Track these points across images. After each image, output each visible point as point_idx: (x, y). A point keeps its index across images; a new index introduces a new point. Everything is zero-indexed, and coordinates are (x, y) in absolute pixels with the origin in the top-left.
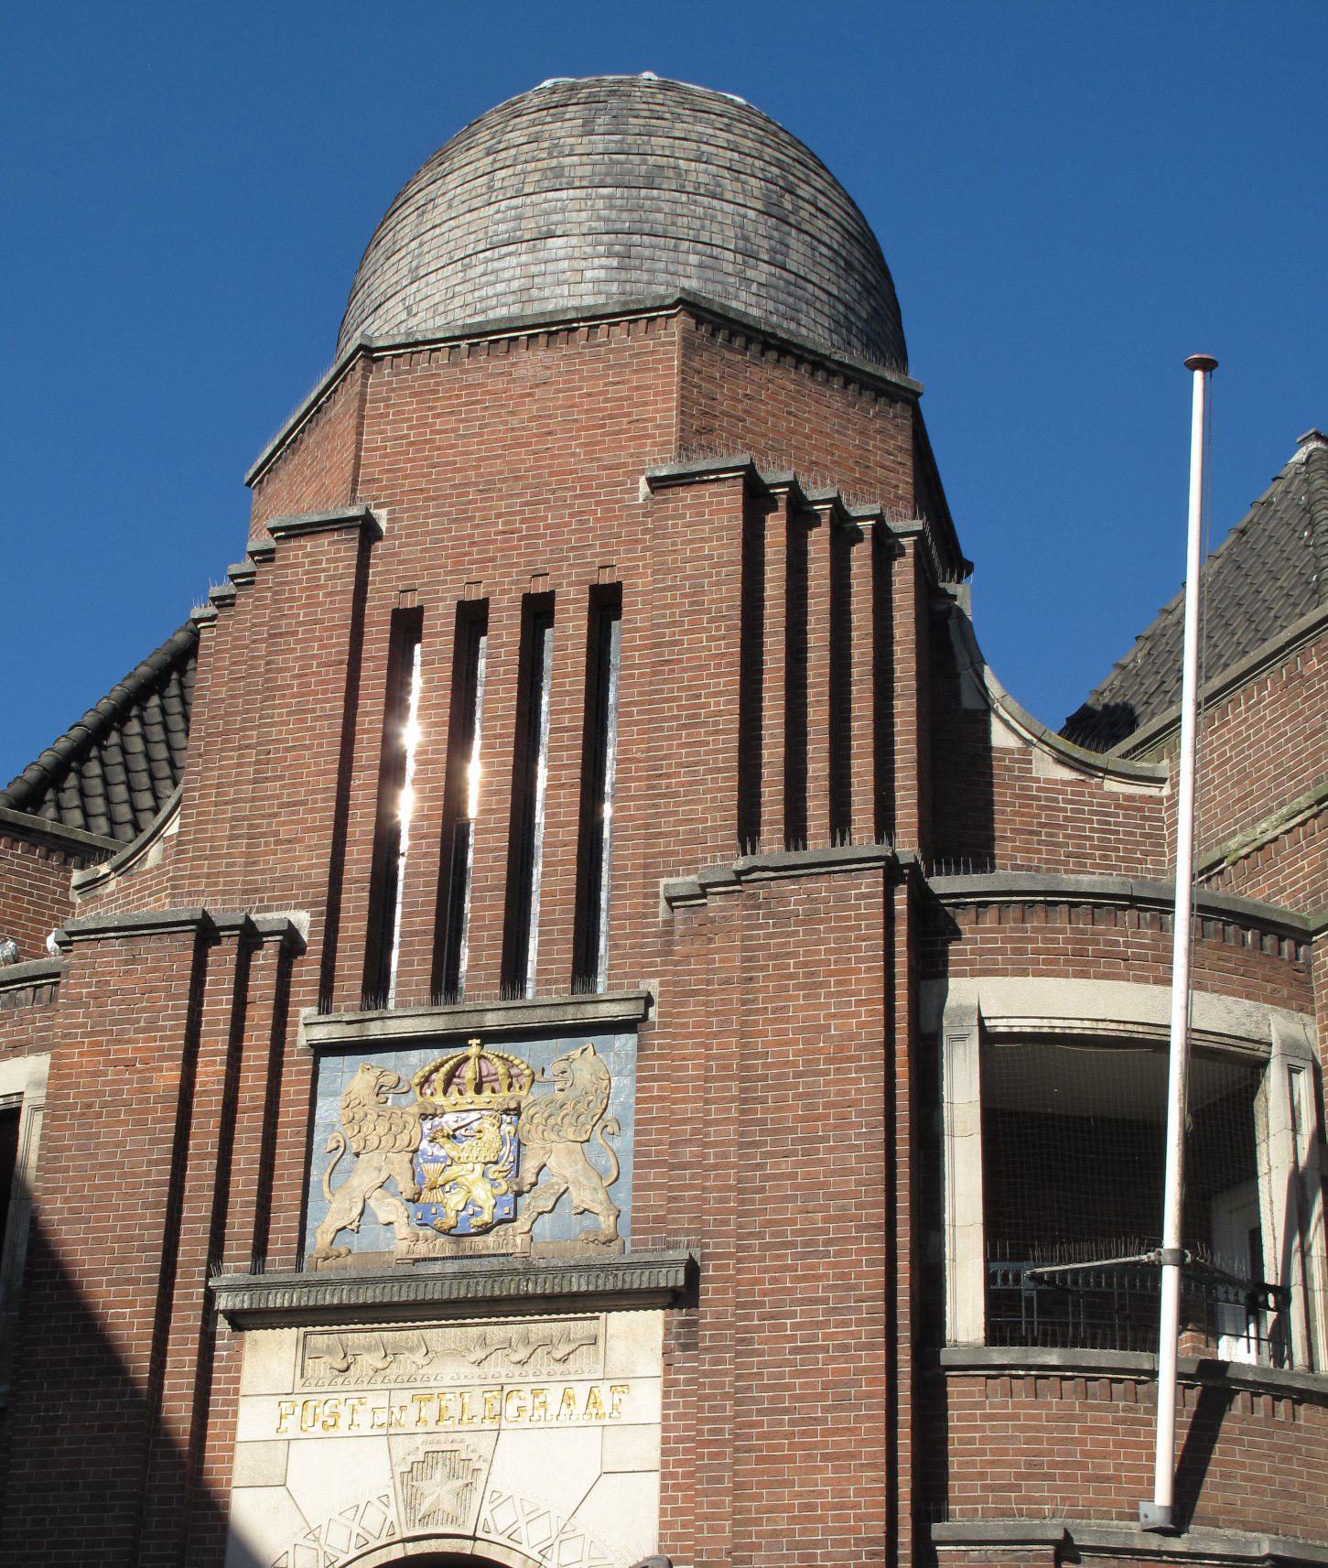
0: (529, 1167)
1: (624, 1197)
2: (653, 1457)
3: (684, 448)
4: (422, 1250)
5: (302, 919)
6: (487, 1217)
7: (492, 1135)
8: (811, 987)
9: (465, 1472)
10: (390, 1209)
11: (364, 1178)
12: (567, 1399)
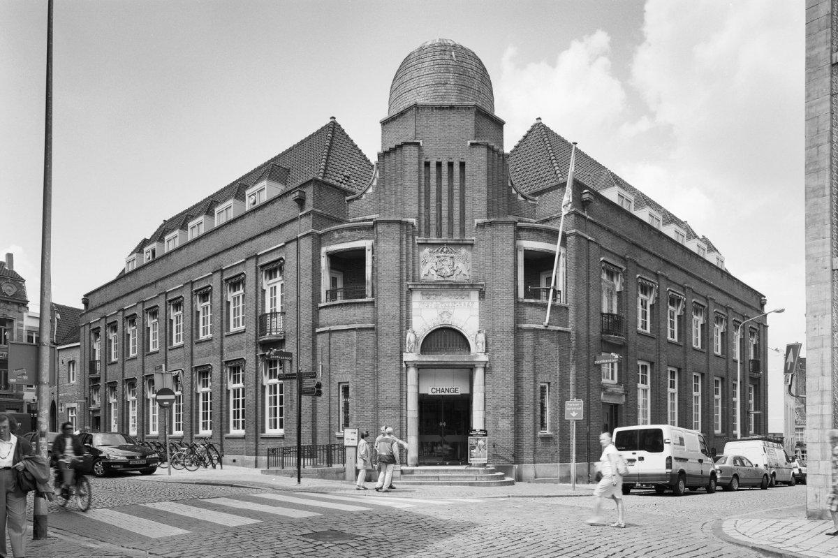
0: (455, 266)
1: (470, 273)
2: (478, 314)
3: (476, 137)
4: (438, 279)
5: (414, 220)
6: (449, 274)
7: (449, 261)
8: (503, 242)
9: (450, 315)
10: (433, 272)
11: (428, 266)
12: (465, 304)
